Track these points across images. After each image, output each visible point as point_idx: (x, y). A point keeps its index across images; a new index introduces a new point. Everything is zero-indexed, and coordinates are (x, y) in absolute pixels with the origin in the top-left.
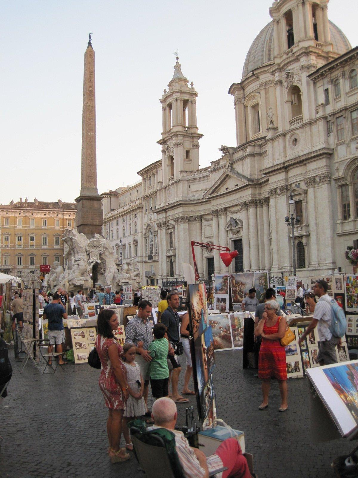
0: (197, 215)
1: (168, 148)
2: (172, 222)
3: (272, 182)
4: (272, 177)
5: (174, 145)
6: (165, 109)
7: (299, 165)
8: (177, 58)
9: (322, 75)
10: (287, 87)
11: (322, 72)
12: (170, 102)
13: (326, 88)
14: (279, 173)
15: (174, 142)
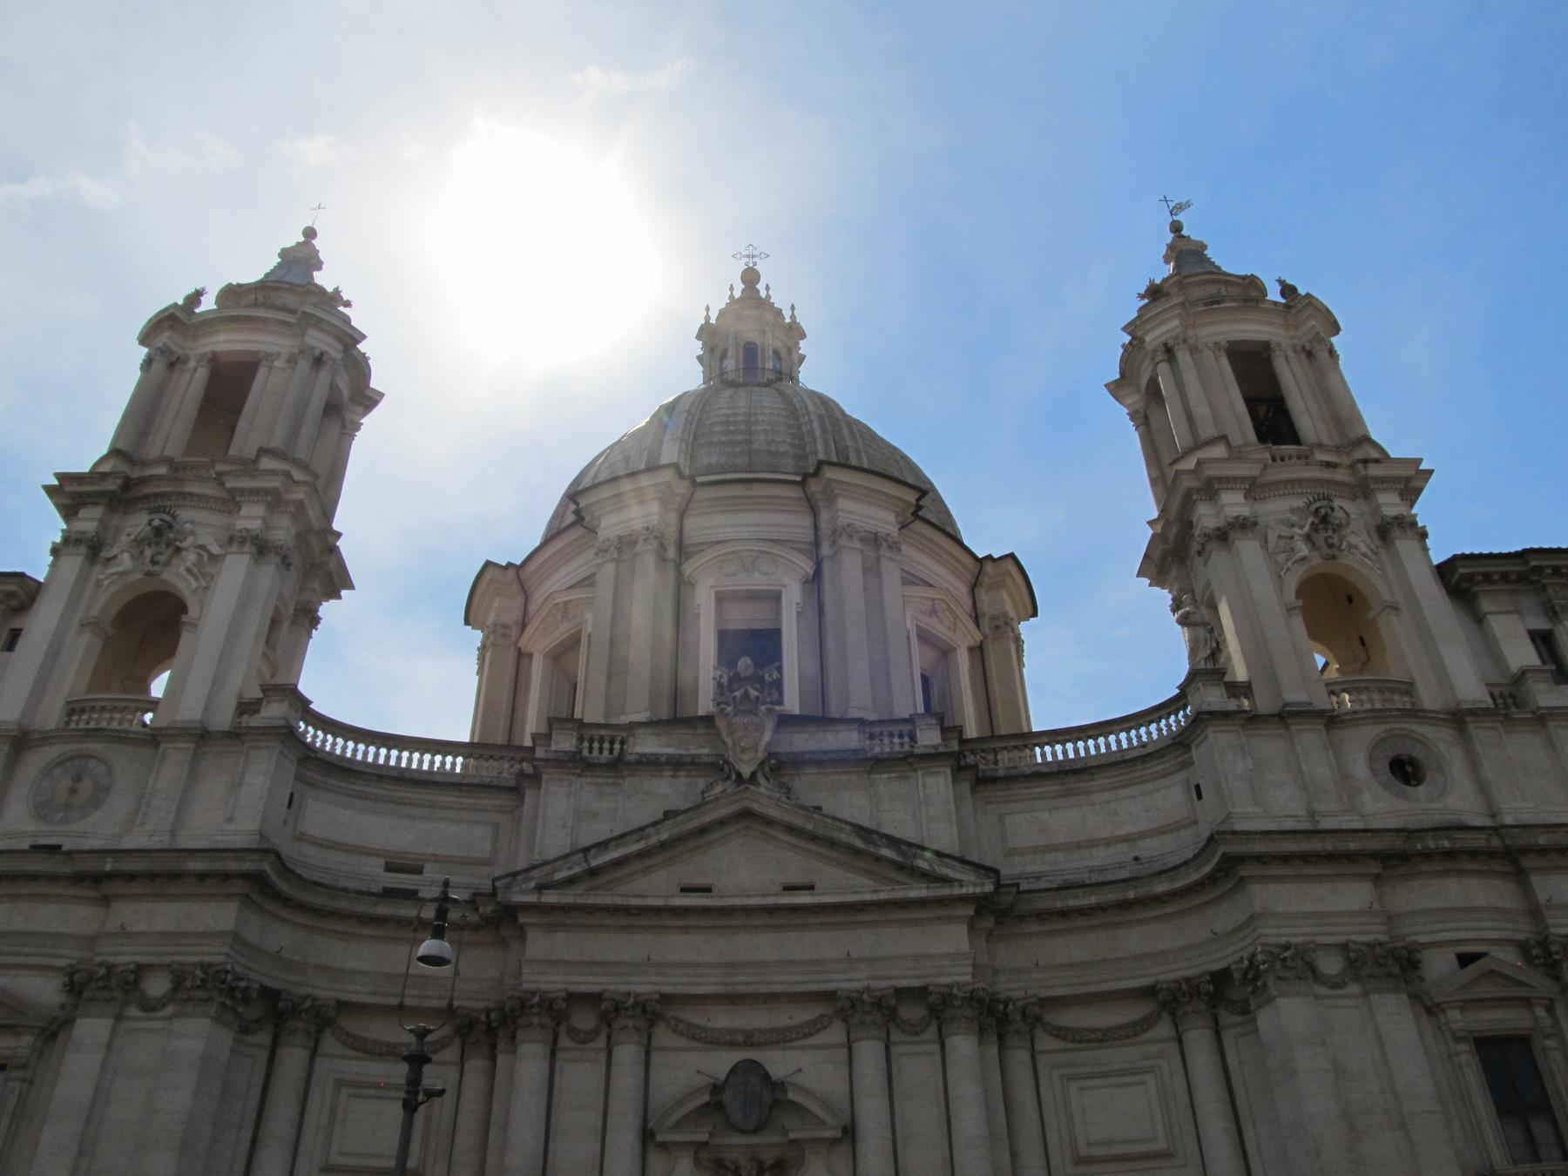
0: (309, 991)
1: (163, 537)
2: (45, 991)
3: (1281, 910)
4: (1273, 887)
5: (235, 540)
6: (172, 365)
7: (1485, 868)
8: (310, 233)
9: (1522, 578)
10: (1303, 559)
11: (1538, 570)
12: (256, 353)
13: (1541, 624)
14: (1339, 876)
15: (241, 524)
